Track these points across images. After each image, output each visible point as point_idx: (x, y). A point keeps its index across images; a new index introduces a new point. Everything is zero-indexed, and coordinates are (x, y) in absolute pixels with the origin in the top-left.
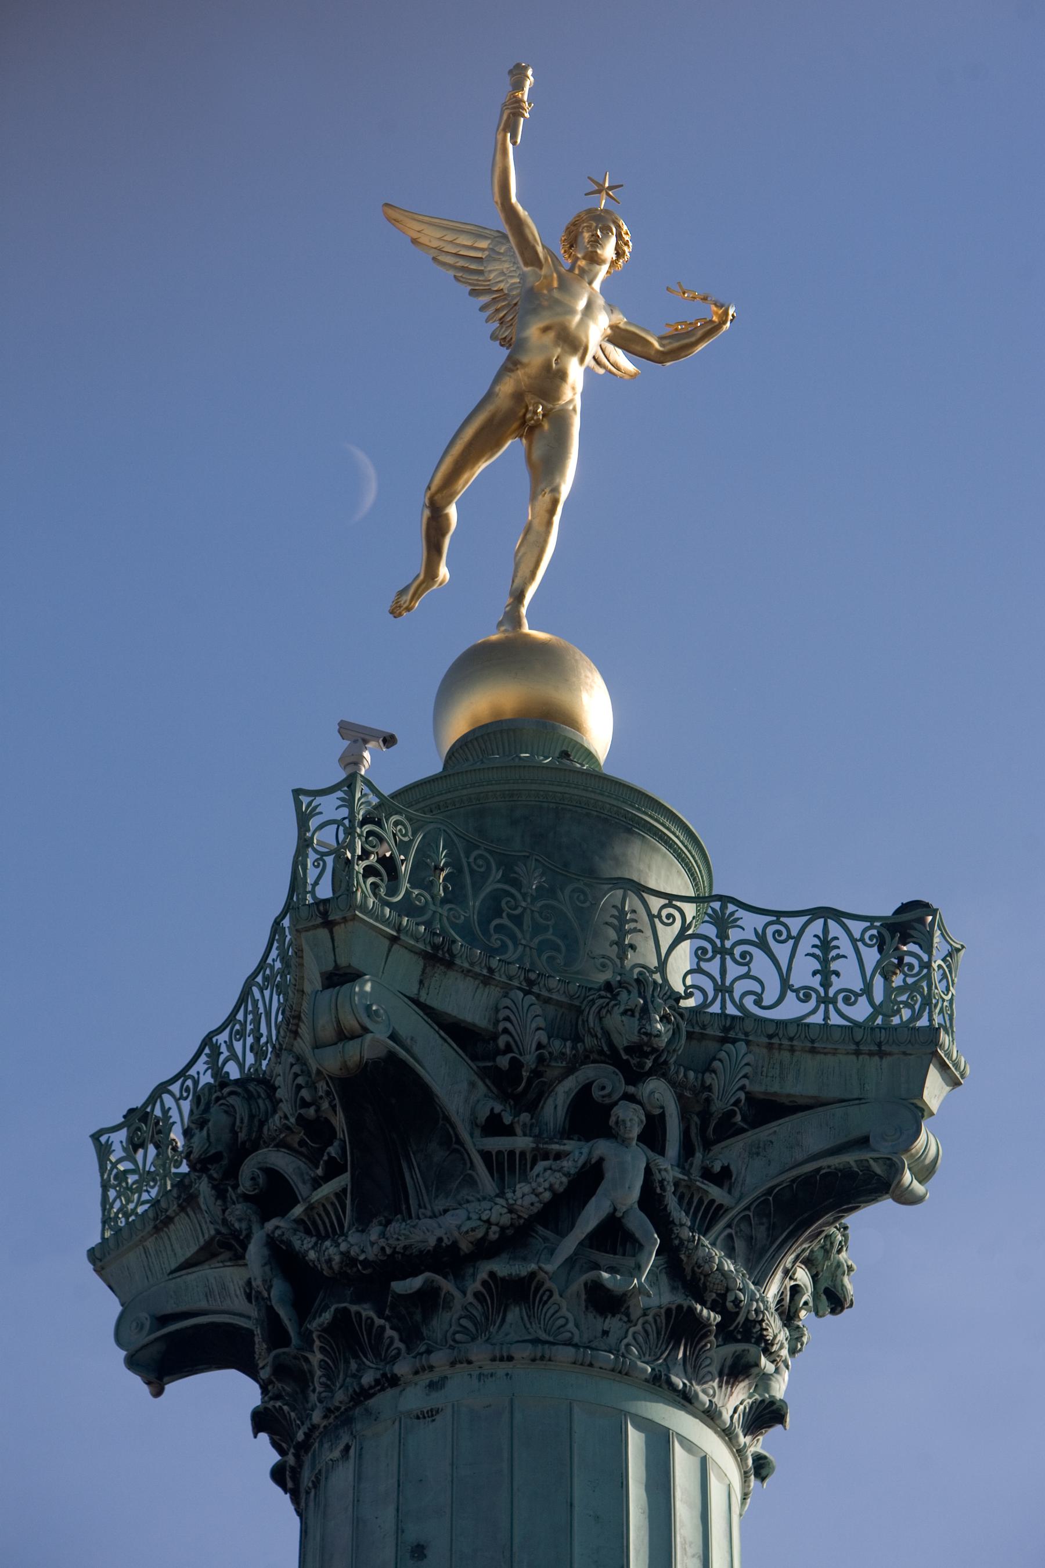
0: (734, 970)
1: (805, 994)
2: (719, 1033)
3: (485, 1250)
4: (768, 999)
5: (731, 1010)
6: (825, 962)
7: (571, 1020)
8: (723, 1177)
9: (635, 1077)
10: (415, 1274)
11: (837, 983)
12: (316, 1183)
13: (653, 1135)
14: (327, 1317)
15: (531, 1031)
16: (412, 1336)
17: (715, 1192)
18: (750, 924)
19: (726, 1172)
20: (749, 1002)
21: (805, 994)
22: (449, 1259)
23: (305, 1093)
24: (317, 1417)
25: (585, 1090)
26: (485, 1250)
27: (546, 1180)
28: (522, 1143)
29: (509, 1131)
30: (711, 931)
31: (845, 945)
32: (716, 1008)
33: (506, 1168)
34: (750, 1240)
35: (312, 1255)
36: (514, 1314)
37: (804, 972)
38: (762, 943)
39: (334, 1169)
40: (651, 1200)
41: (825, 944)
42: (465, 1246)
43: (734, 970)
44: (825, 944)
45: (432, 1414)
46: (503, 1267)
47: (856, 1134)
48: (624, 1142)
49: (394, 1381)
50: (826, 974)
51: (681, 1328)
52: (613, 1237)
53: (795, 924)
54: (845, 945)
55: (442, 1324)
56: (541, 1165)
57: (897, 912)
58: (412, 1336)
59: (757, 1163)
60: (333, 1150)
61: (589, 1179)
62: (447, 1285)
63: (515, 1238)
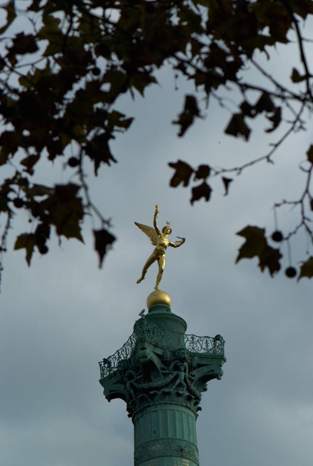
0: (195, 346)
1: (204, 349)
2: (193, 355)
3: (163, 387)
4: (199, 350)
5: (194, 352)
6: (207, 344)
7: (174, 353)
8: (193, 376)
9: (183, 362)
10: (153, 391)
11: (209, 348)
12: (137, 376)
13: (185, 371)
14: (140, 396)
15: (169, 355)
16: (152, 399)
17: (193, 378)
18: (196, 339)
19: (194, 375)
20: (197, 350)
21: (204, 349)
22: (158, 388)
23: (136, 363)
24: (138, 410)
25: (176, 364)
26: (163, 387)
27: (171, 377)
28: (167, 372)
29: (165, 370)
30: (191, 340)
31: (209, 341)
32: (192, 351)
33: (165, 375)
34: (197, 384)
35: (137, 386)
36: (167, 397)
37: (204, 346)
38: (198, 342)
39: (140, 374)
40: (185, 380)
41: (207, 342)
42: (160, 387)
43: (195, 346)
44: (207, 342)
45: (155, 411)
46: (166, 390)
47: (212, 369)
48: (181, 372)
49: (149, 406)
50: (207, 346)
51: (189, 399)
52: (180, 385)
53: (203, 338)
54: (209, 342)
55: (156, 398)
56: (170, 375)
57: (216, 337)
58: (152, 399)
59: (197, 374)
60: (140, 371)
61: (177, 377)
62: (157, 392)
63: (166, 385)
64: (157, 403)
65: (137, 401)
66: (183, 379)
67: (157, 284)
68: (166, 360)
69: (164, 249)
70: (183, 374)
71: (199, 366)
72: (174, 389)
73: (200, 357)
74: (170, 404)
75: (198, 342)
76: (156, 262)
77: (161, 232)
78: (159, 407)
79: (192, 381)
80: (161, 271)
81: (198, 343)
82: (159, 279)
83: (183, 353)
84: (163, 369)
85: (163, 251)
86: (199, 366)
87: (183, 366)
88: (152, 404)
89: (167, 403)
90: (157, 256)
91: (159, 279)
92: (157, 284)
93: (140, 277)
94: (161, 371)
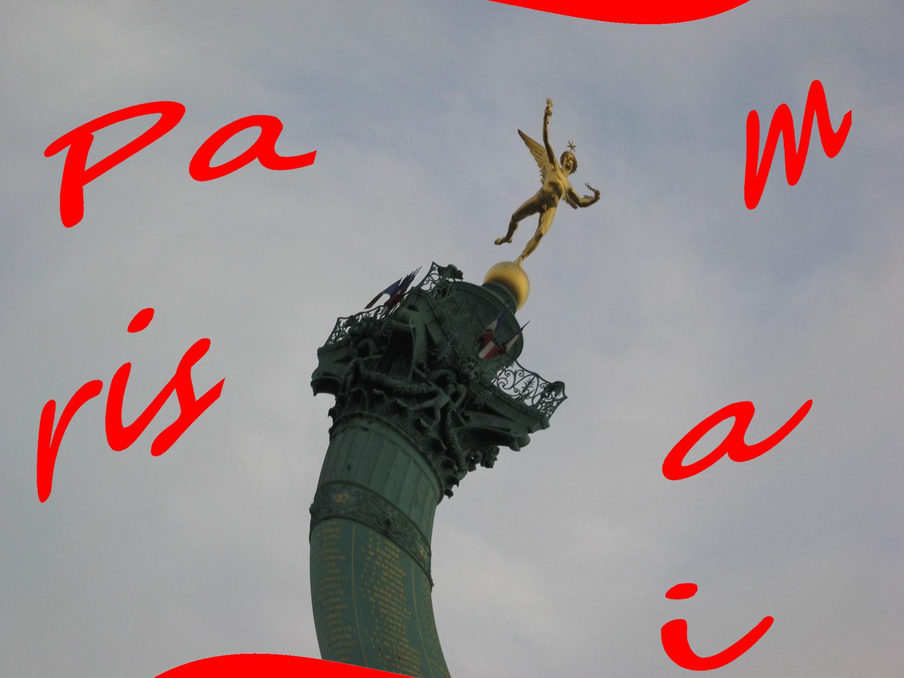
3: (399, 395)
5: (495, 384)
8: (467, 418)
10: (380, 389)
13: (455, 396)
16: (372, 406)
17: (462, 420)
20: (501, 385)
22: (390, 391)
26: (399, 395)
27: (423, 388)
28: (424, 375)
29: (423, 371)
33: (417, 379)
36: (396, 416)
37: (520, 386)
38: (515, 374)
39: (380, 352)
40: (444, 410)
41: (530, 382)
44: (530, 382)
45: (365, 430)
46: (400, 402)
48: (447, 393)
49: (361, 415)
53: (526, 374)
54: (535, 385)
61: (433, 395)
62: (386, 398)
63: (409, 396)
64: (375, 415)
65: (349, 399)
66: (442, 405)
67: (523, 257)
68: (435, 357)
69: (557, 198)
70: (444, 399)
71: (488, 410)
72: (416, 412)
73: (498, 397)
74: (396, 431)
75: (515, 374)
76: (537, 215)
77: (557, 157)
78: (375, 426)
79: (459, 424)
80: (538, 237)
81: (512, 375)
82: (529, 250)
83: (469, 367)
84: (420, 367)
85: (554, 199)
86: (488, 410)
87: (455, 385)
88: (366, 413)
89: (389, 426)
90: (541, 204)
91: (529, 250)
92: (523, 257)
93: (504, 234)
94: (414, 368)
